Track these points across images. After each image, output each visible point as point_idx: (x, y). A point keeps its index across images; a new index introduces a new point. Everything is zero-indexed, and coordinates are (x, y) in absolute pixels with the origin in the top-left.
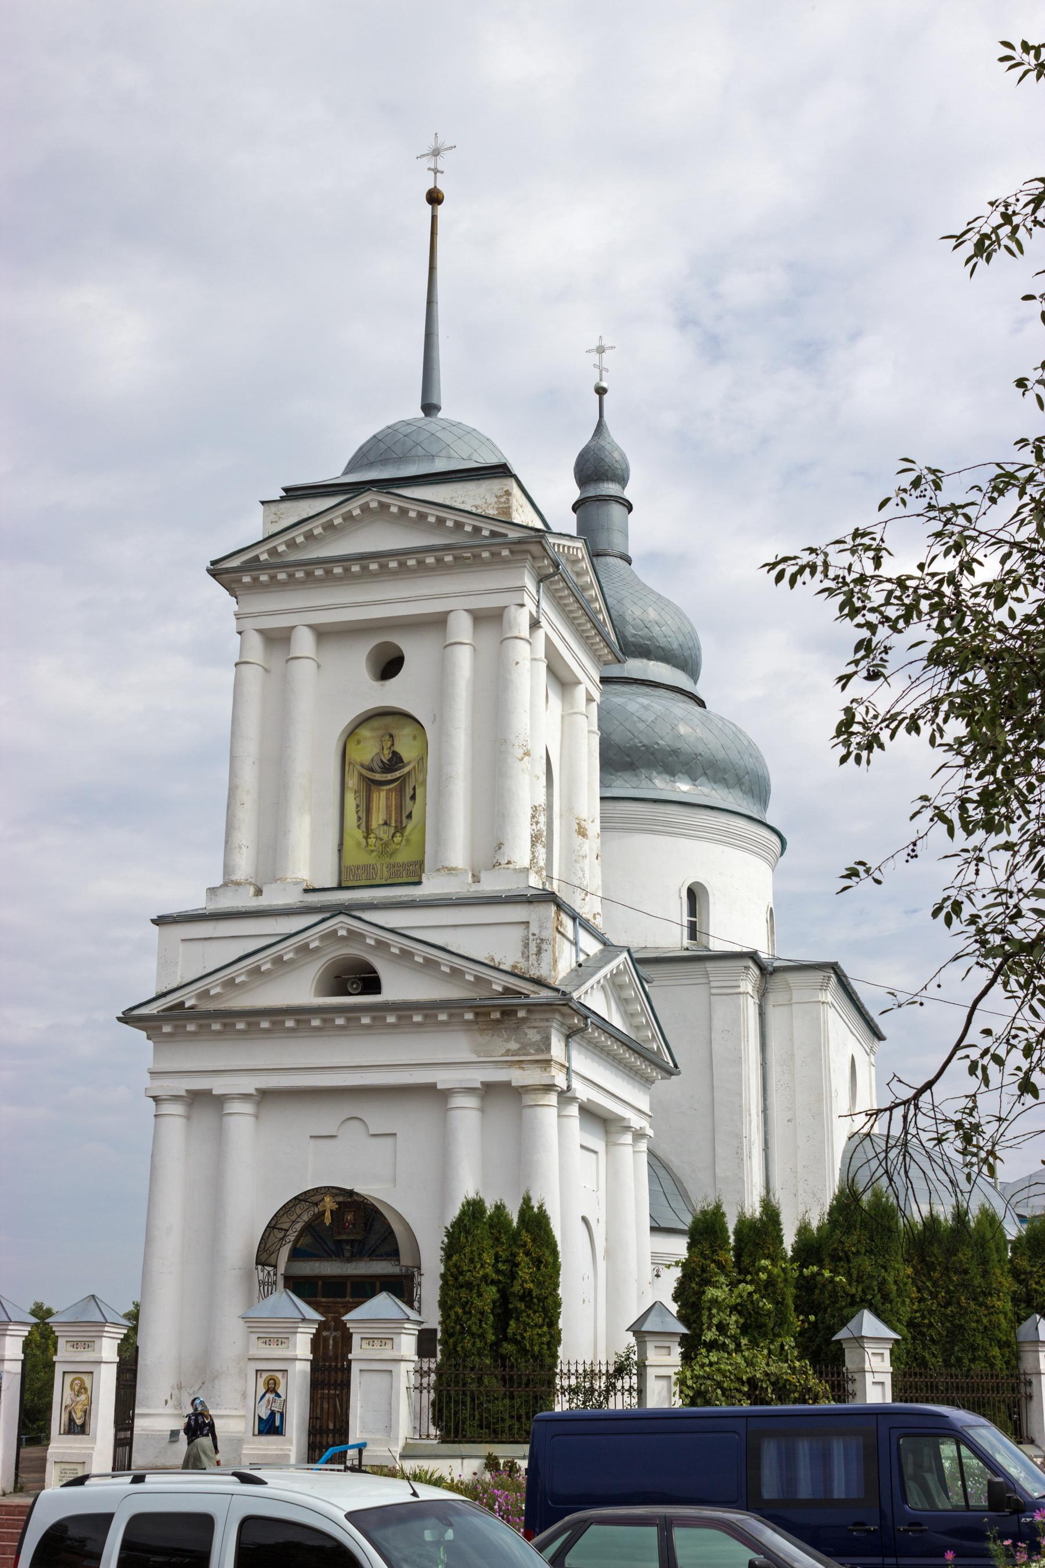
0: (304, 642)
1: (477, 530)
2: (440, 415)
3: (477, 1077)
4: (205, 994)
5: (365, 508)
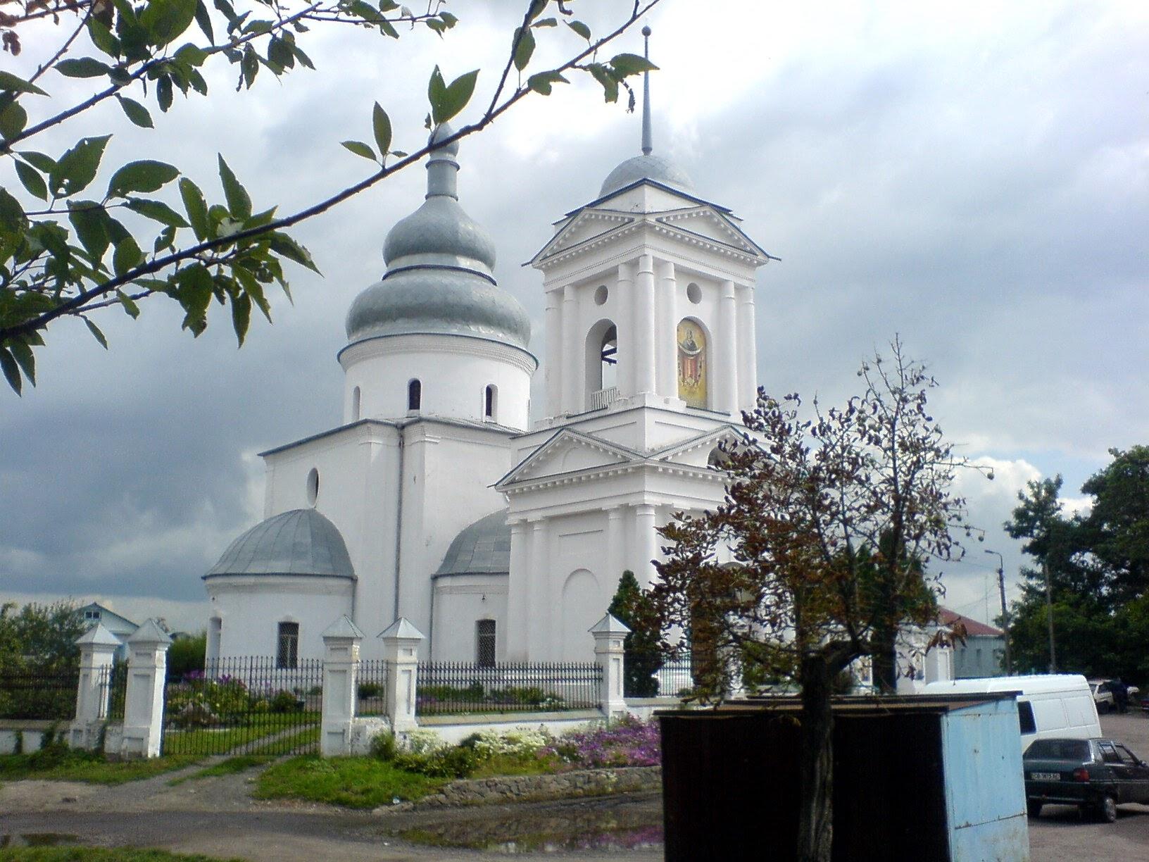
0: (568, 293)
1: (623, 219)
2: (652, 153)
3: (615, 504)
4: (522, 473)
5: (585, 220)
